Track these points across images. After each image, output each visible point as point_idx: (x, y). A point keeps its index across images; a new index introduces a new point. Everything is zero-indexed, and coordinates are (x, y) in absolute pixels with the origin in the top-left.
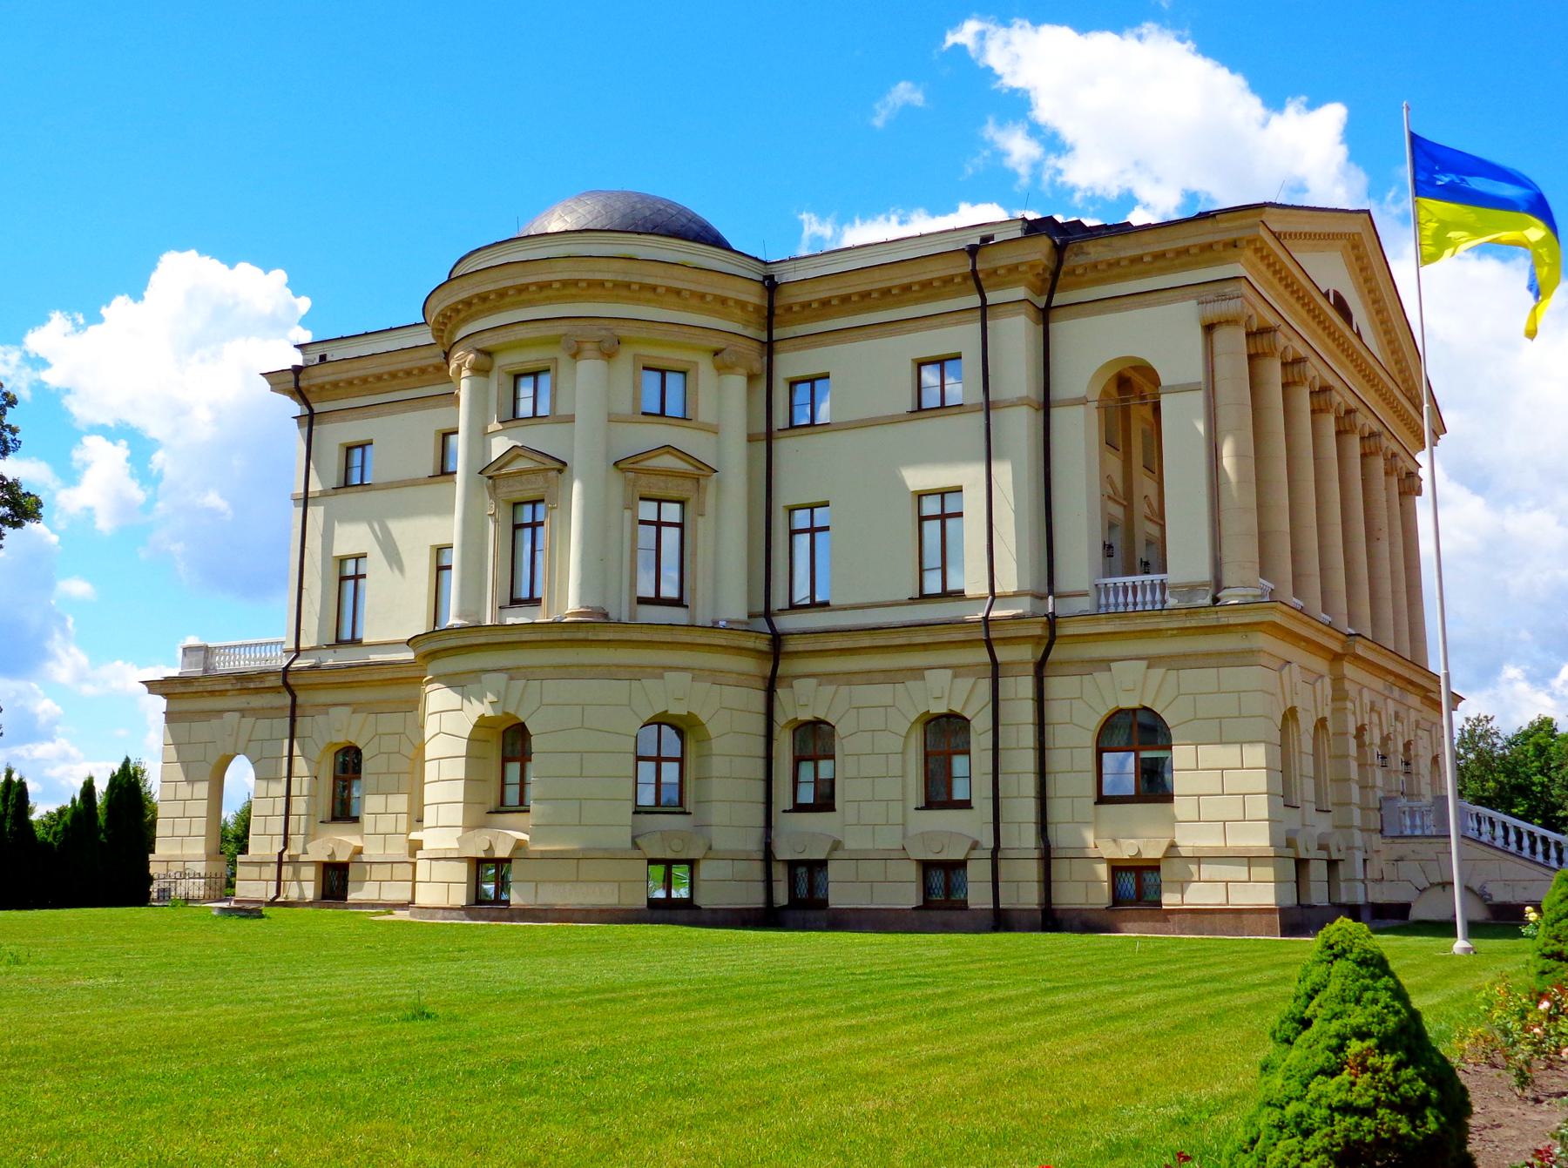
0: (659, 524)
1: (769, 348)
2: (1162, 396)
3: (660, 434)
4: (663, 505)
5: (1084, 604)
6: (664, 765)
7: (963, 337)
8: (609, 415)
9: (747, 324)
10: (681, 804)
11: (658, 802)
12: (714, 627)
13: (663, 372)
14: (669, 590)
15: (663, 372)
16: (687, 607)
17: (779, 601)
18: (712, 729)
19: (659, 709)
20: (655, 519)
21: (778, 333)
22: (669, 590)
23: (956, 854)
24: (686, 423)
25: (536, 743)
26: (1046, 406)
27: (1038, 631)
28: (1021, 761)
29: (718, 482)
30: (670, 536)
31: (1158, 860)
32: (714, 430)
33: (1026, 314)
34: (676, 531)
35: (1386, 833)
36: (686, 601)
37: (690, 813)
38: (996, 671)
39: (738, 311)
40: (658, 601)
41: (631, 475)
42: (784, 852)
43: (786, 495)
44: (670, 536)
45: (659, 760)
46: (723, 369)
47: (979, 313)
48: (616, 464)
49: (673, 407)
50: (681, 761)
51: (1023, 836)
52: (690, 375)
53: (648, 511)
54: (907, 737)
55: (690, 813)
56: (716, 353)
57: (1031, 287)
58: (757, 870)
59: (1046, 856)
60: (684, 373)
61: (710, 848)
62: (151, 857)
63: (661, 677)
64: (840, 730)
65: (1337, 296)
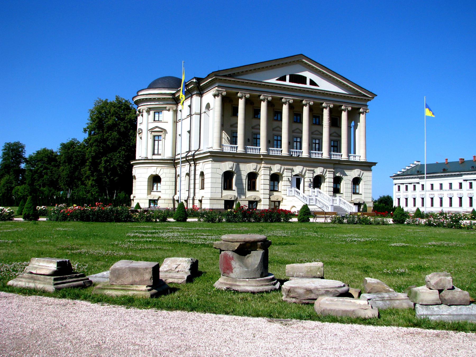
0: (158, 141)
9: (173, 101)
27: (191, 158)
35: (287, 195)
38: (190, 166)
40: (158, 154)
51: (192, 196)
59: (193, 199)
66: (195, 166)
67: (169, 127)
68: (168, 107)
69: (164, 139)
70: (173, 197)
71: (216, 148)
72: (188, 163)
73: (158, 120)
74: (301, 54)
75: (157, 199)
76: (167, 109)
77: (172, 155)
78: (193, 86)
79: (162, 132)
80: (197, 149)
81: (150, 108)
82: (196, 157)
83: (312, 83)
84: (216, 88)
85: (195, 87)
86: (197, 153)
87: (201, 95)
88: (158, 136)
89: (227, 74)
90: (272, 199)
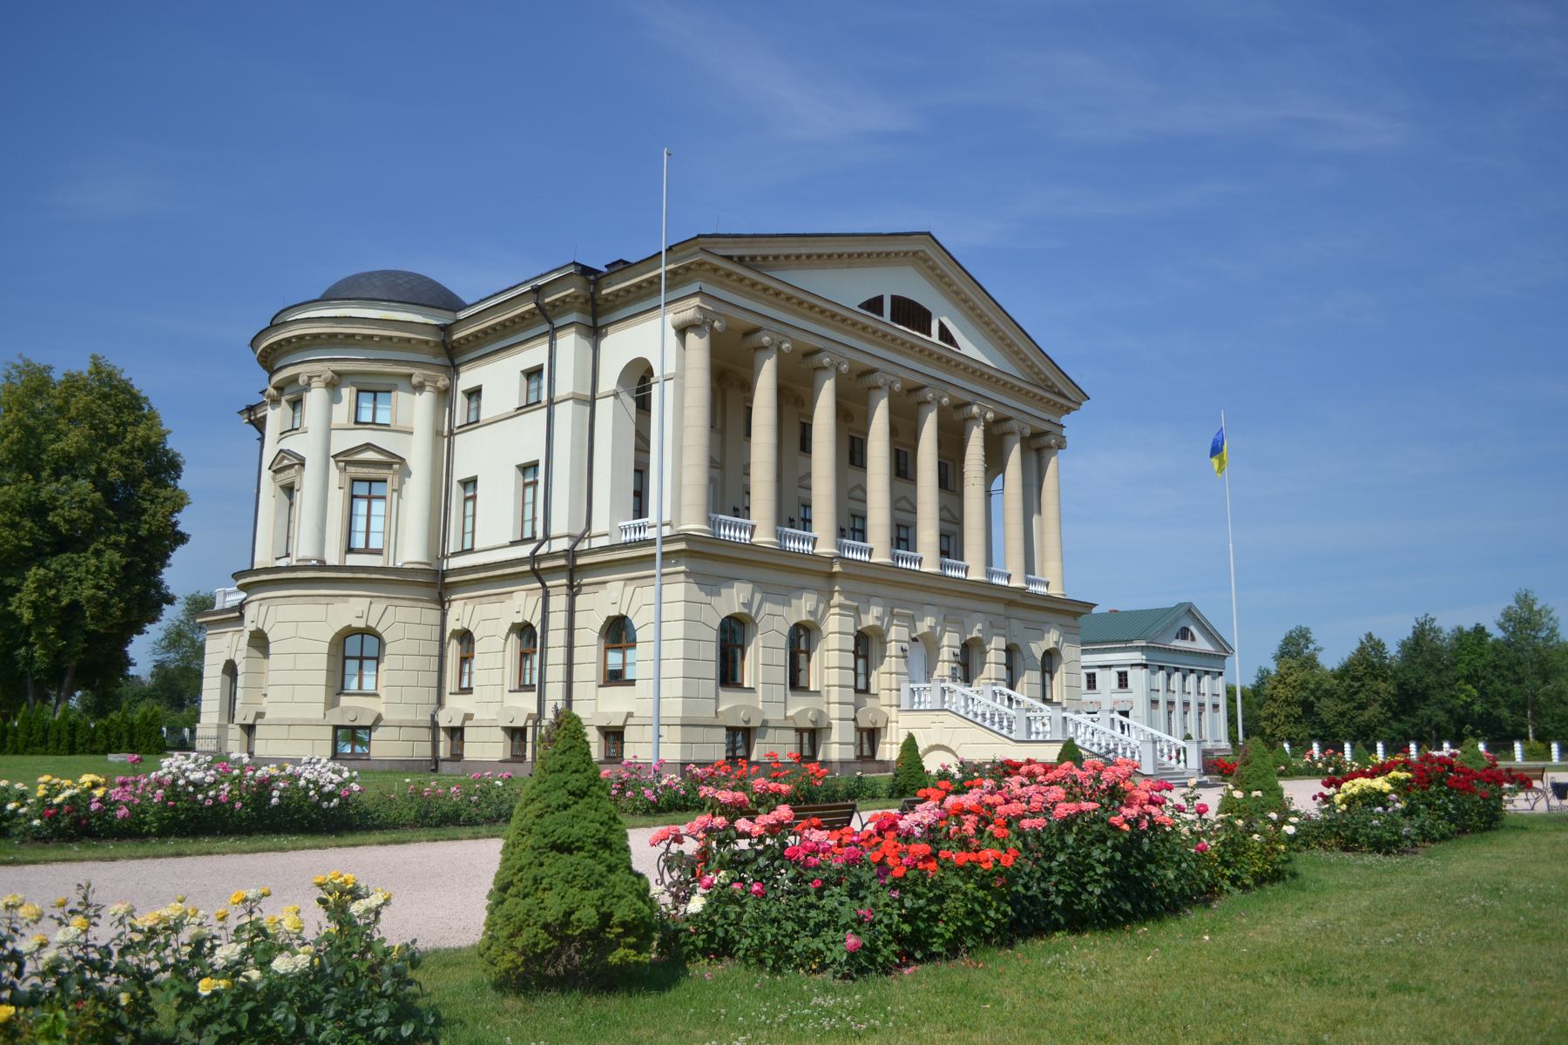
0: (370, 498)
1: (453, 369)
2: (653, 386)
3: (363, 437)
5: (604, 542)
6: (365, 662)
7: (535, 354)
9: (436, 356)
13: (375, 392)
15: (375, 392)
17: (453, 547)
18: (386, 637)
20: (366, 493)
21: (457, 362)
22: (375, 543)
23: (519, 723)
25: (273, 648)
26: (591, 402)
27: (562, 562)
28: (556, 656)
31: (623, 727)
33: (578, 332)
35: (902, 708)
39: (425, 347)
40: (367, 550)
42: (443, 721)
43: (460, 473)
45: (361, 659)
46: (420, 388)
47: (547, 339)
53: (361, 489)
54: (506, 639)
56: (410, 376)
57: (582, 311)
58: (426, 734)
62: (198, 725)
63: (348, 602)
64: (476, 636)
65: (895, 299)
66: (572, 597)
67: (417, 452)
68: (418, 375)
69: (395, 494)
70: (433, 717)
71: (693, 523)
72: (539, 585)
74: (929, 234)
75: (369, 723)
76: (415, 380)
77: (429, 555)
78: (573, 290)
79: (389, 465)
80: (579, 532)
81: (339, 374)
82: (580, 561)
83: (945, 335)
84: (696, 301)
85: (576, 297)
86: (584, 545)
87: (595, 332)
88: (370, 481)
89: (735, 252)
90: (862, 724)
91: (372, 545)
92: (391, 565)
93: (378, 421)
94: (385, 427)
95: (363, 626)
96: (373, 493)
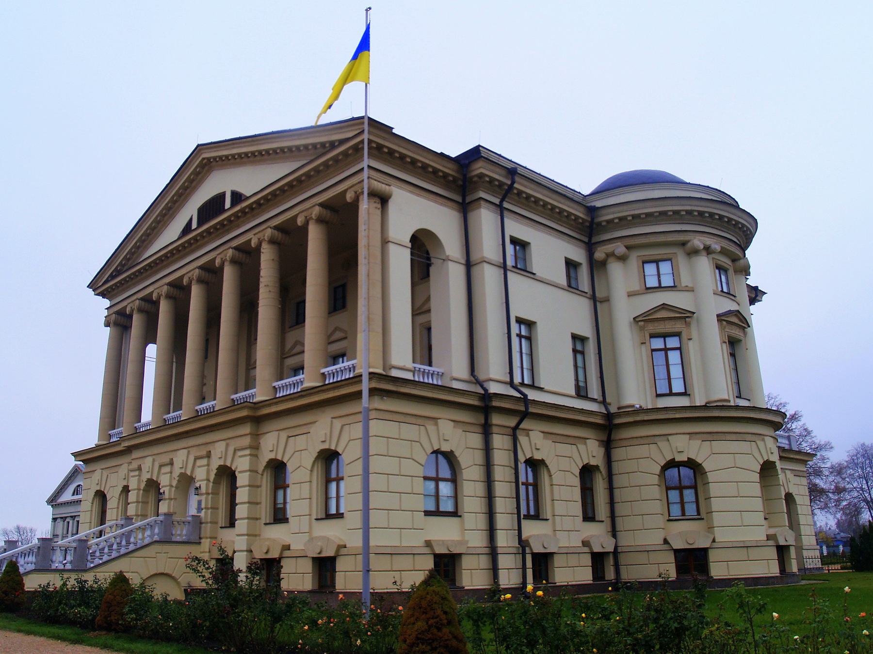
0: (666, 350)
4: (667, 339)
8: (628, 293)
10: (699, 513)
11: (683, 514)
12: (705, 407)
13: (657, 262)
14: (678, 387)
16: (689, 395)
18: (707, 466)
19: (669, 458)
20: (663, 347)
24: (673, 289)
29: (698, 321)
30: (674, 357)
32: (692, 290)
34: (678, 352)
36: (688, 393)
37: (703, 519)
40: (671, 394)
41: (642, 323)
44: (674, 357)
48: (634, 318)
49: (667, 281)
50: (695, 487)
52: (673, 260)
53: (658, 343)
55: (703, 519)
60: (670, 260)
61: (714, 541)
73: (657, 285)
91: (674, 391)
92: (697, 405)
93: (662, 286)
94: (673, 288)
95: (686, 460)
96: (667, 347)
